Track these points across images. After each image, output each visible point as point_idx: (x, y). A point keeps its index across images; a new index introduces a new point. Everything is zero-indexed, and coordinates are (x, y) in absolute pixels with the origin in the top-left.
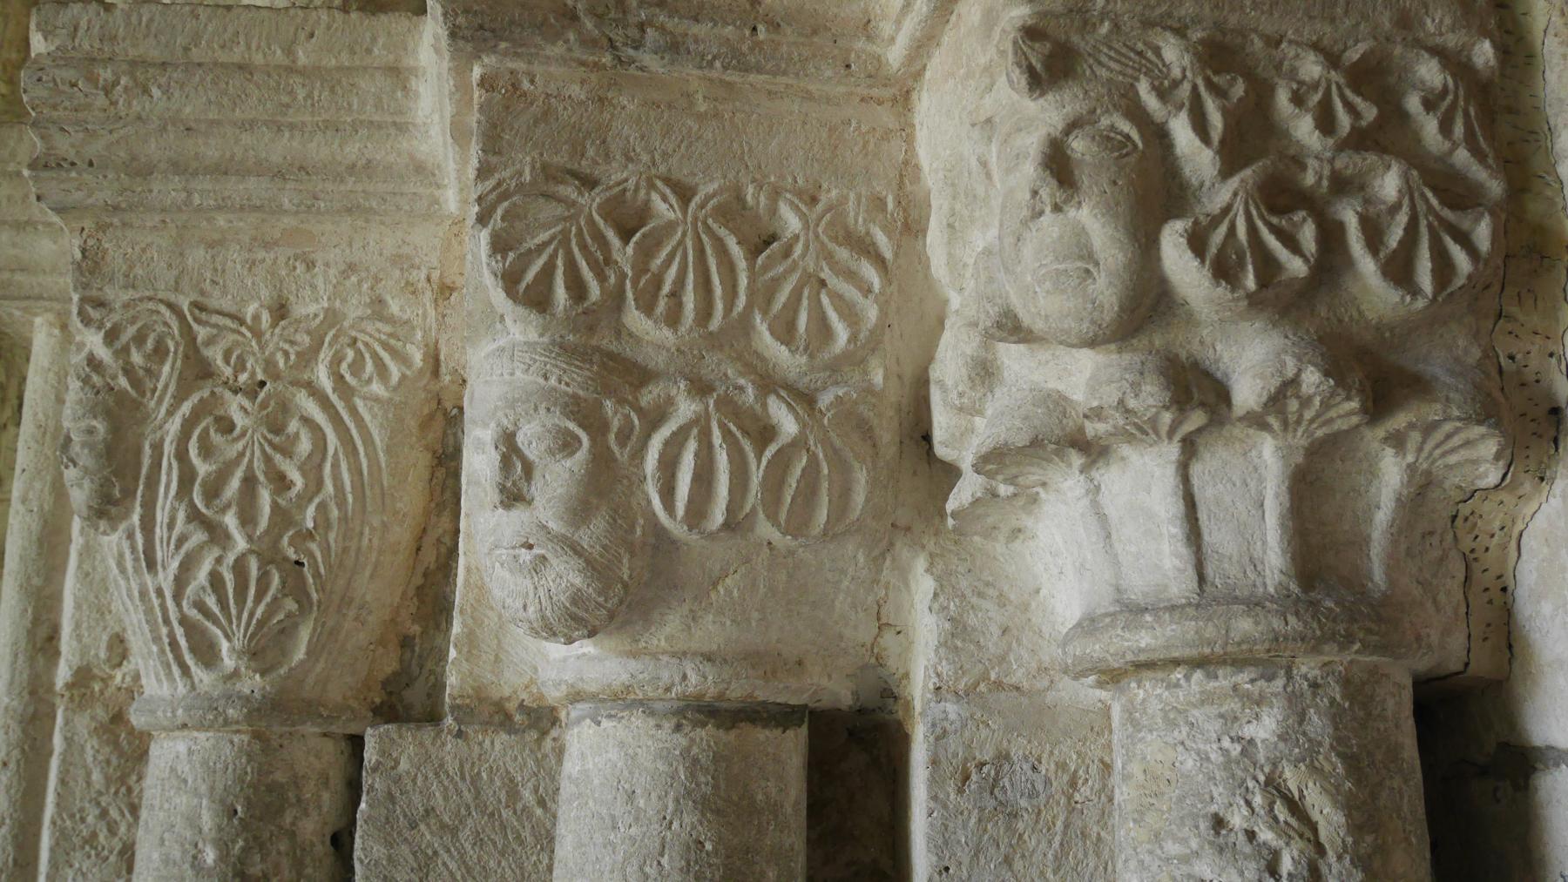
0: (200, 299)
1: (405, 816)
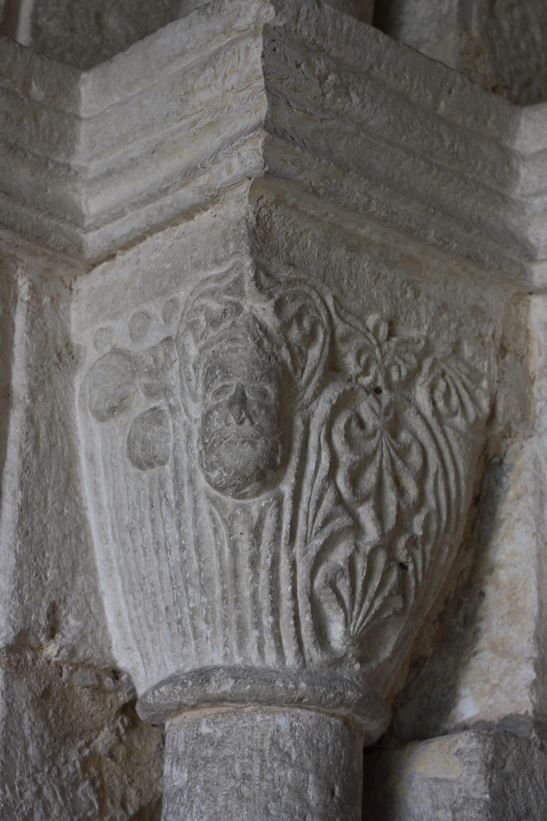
0: (339, 295)
1: (514, 812)
